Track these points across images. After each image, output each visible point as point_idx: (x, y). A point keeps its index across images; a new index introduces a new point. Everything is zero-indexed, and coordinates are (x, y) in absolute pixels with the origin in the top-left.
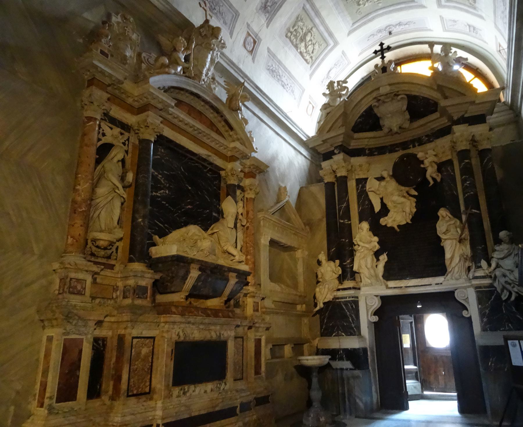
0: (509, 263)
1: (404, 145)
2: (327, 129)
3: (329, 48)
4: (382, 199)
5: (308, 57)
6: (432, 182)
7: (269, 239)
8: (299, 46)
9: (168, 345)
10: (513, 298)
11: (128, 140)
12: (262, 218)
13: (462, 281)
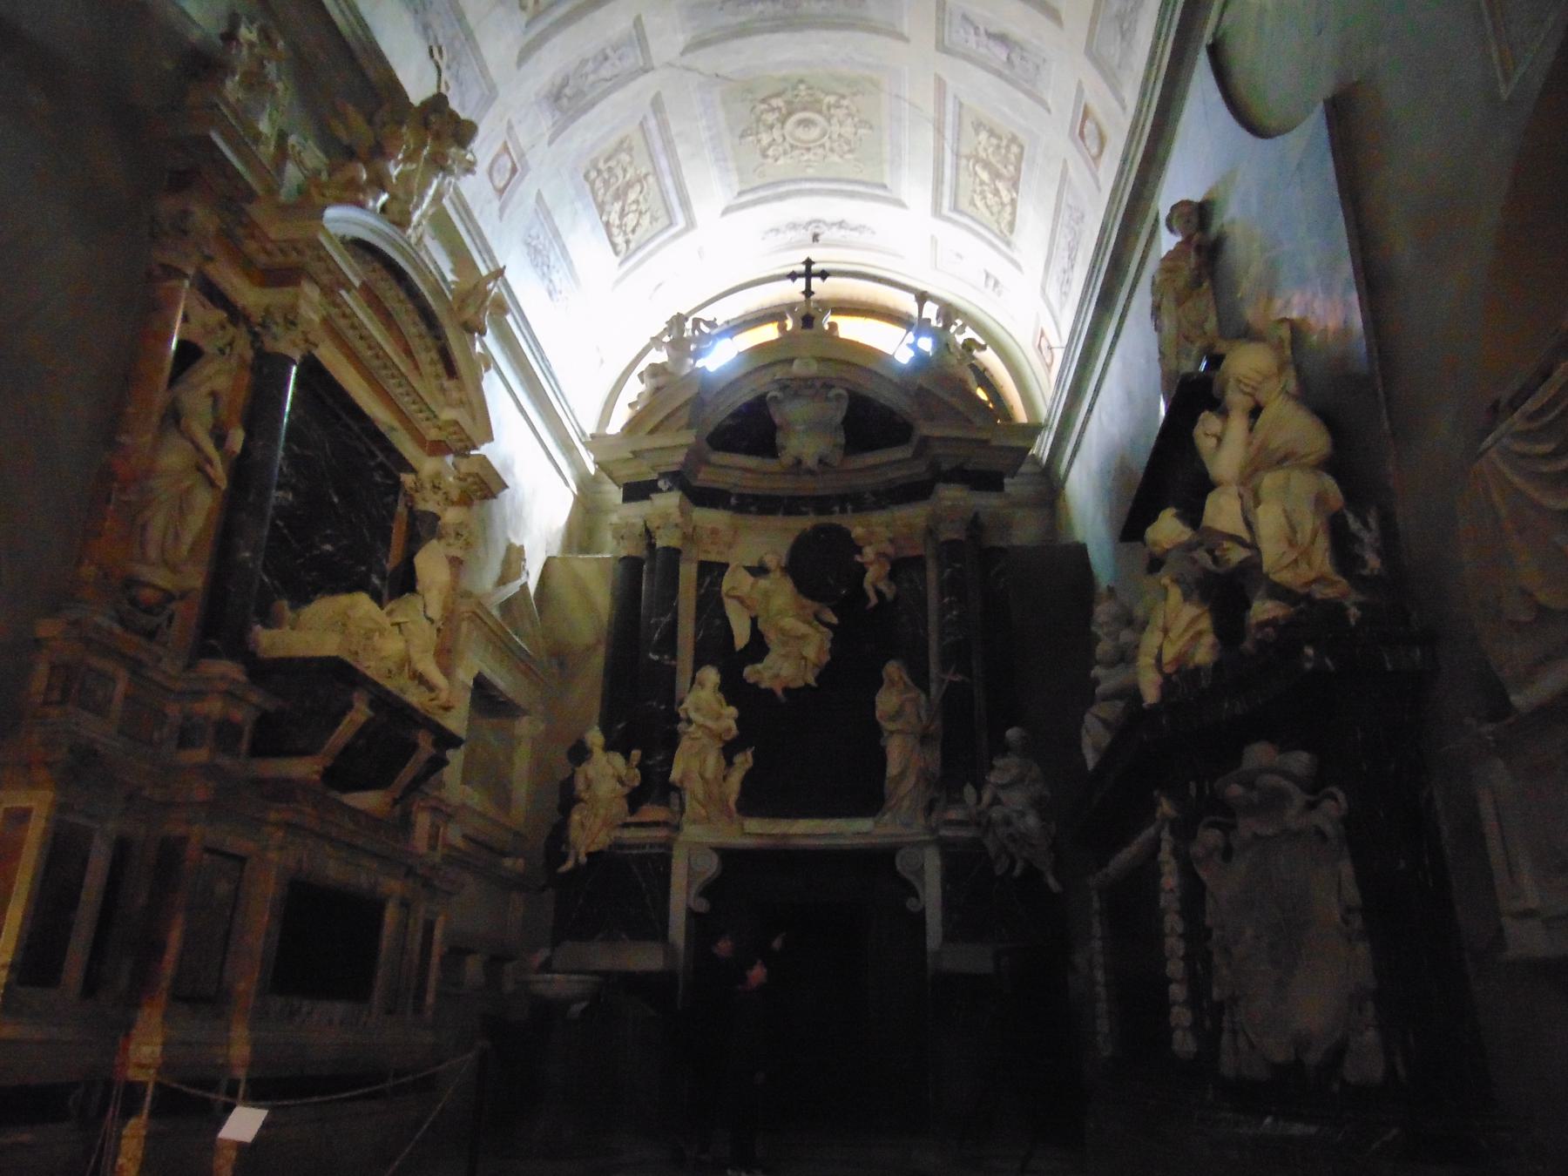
0: (1016, 799)
1: (821, 504)
2: (650, 425)
3: (673, 230)
4: (754, 621)
5: (620, 240)
6: (874, 600)
8: (607, 208)
10: (1017, 872)
11: (230, 344)
12: (466, 615)
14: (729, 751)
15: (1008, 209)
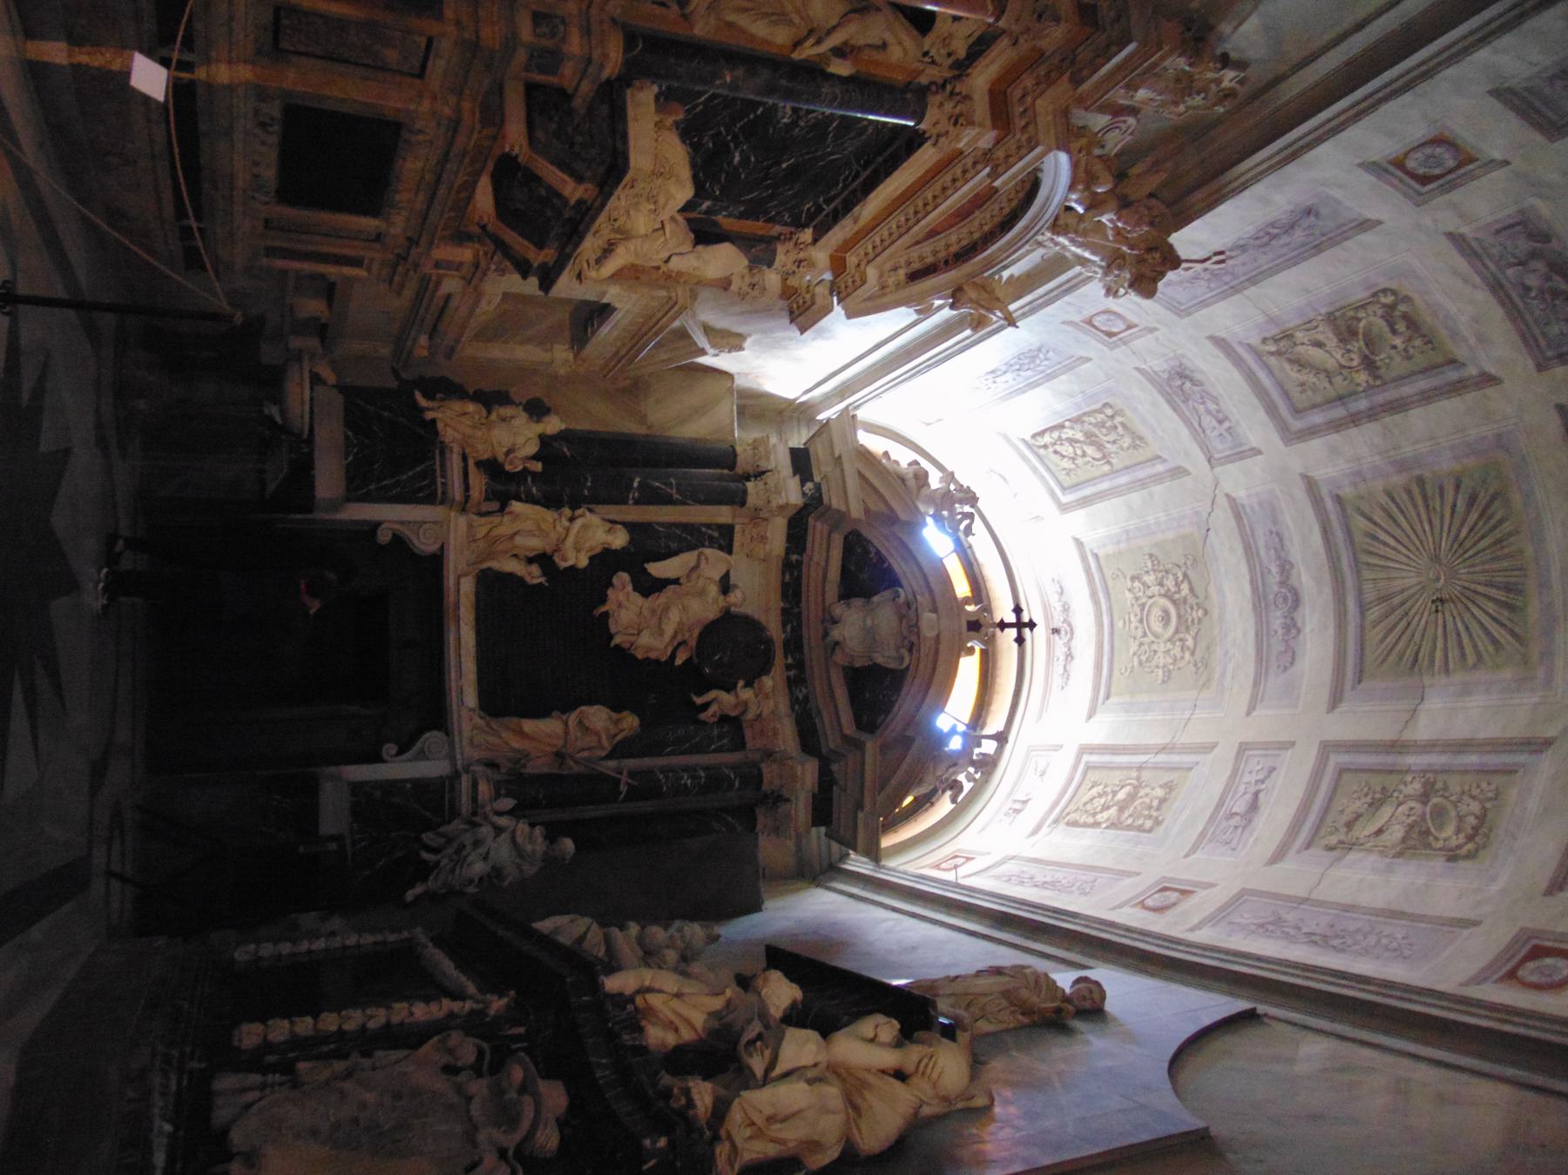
0: (502, 851)
1: (794, 644)
2: (868, 474)
3: (1058, 491)
4: (676, 581)
5: (1047, 439)
6: (699, 701)
7: (617, 305)
8: (1078, 427)
9: (398, 110)
10: (425, 855)
11: (933, 62)
12: (674, 295)
13: (468, 751)
14: (543, 560)
15: (1090, 820)
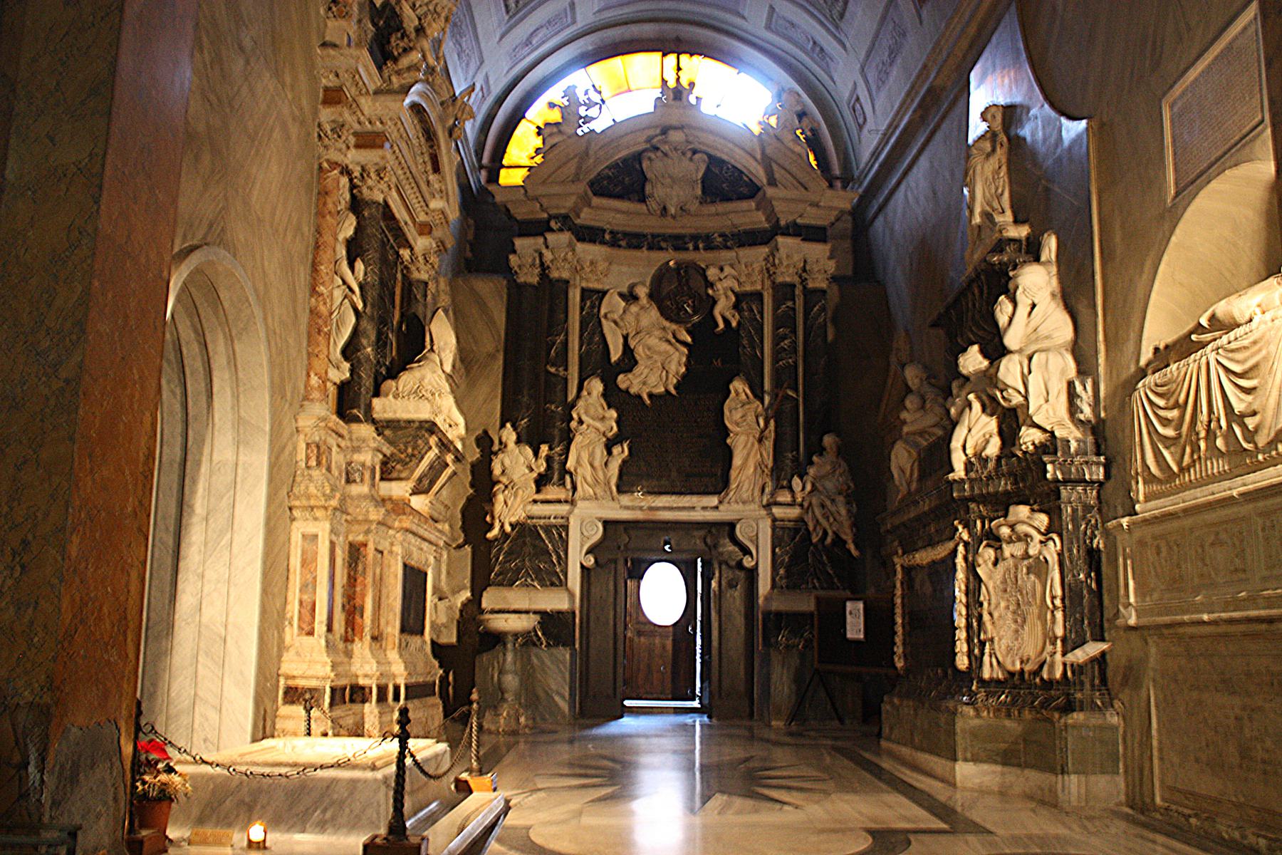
1: (678, 242)
4: (626, 338)
6: (721, 325)
10: (829, 540)
